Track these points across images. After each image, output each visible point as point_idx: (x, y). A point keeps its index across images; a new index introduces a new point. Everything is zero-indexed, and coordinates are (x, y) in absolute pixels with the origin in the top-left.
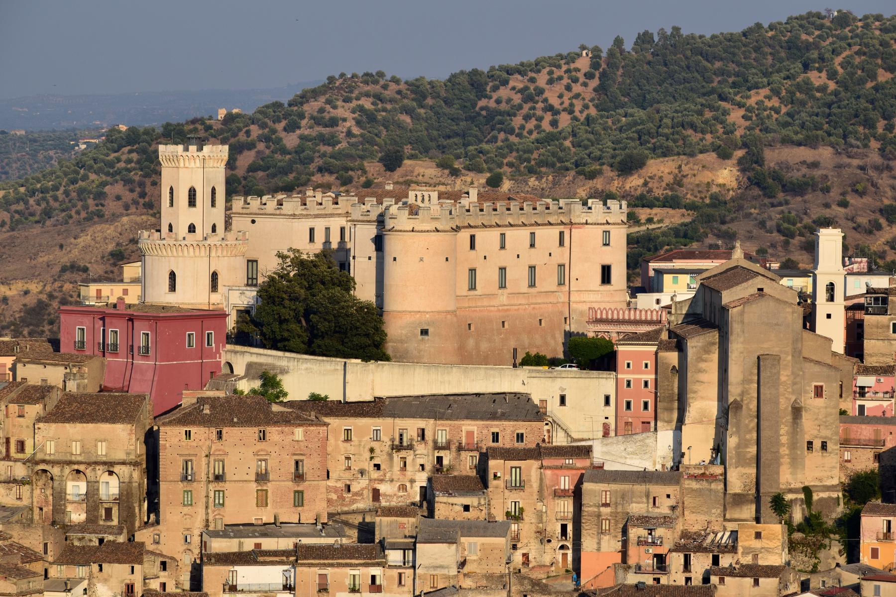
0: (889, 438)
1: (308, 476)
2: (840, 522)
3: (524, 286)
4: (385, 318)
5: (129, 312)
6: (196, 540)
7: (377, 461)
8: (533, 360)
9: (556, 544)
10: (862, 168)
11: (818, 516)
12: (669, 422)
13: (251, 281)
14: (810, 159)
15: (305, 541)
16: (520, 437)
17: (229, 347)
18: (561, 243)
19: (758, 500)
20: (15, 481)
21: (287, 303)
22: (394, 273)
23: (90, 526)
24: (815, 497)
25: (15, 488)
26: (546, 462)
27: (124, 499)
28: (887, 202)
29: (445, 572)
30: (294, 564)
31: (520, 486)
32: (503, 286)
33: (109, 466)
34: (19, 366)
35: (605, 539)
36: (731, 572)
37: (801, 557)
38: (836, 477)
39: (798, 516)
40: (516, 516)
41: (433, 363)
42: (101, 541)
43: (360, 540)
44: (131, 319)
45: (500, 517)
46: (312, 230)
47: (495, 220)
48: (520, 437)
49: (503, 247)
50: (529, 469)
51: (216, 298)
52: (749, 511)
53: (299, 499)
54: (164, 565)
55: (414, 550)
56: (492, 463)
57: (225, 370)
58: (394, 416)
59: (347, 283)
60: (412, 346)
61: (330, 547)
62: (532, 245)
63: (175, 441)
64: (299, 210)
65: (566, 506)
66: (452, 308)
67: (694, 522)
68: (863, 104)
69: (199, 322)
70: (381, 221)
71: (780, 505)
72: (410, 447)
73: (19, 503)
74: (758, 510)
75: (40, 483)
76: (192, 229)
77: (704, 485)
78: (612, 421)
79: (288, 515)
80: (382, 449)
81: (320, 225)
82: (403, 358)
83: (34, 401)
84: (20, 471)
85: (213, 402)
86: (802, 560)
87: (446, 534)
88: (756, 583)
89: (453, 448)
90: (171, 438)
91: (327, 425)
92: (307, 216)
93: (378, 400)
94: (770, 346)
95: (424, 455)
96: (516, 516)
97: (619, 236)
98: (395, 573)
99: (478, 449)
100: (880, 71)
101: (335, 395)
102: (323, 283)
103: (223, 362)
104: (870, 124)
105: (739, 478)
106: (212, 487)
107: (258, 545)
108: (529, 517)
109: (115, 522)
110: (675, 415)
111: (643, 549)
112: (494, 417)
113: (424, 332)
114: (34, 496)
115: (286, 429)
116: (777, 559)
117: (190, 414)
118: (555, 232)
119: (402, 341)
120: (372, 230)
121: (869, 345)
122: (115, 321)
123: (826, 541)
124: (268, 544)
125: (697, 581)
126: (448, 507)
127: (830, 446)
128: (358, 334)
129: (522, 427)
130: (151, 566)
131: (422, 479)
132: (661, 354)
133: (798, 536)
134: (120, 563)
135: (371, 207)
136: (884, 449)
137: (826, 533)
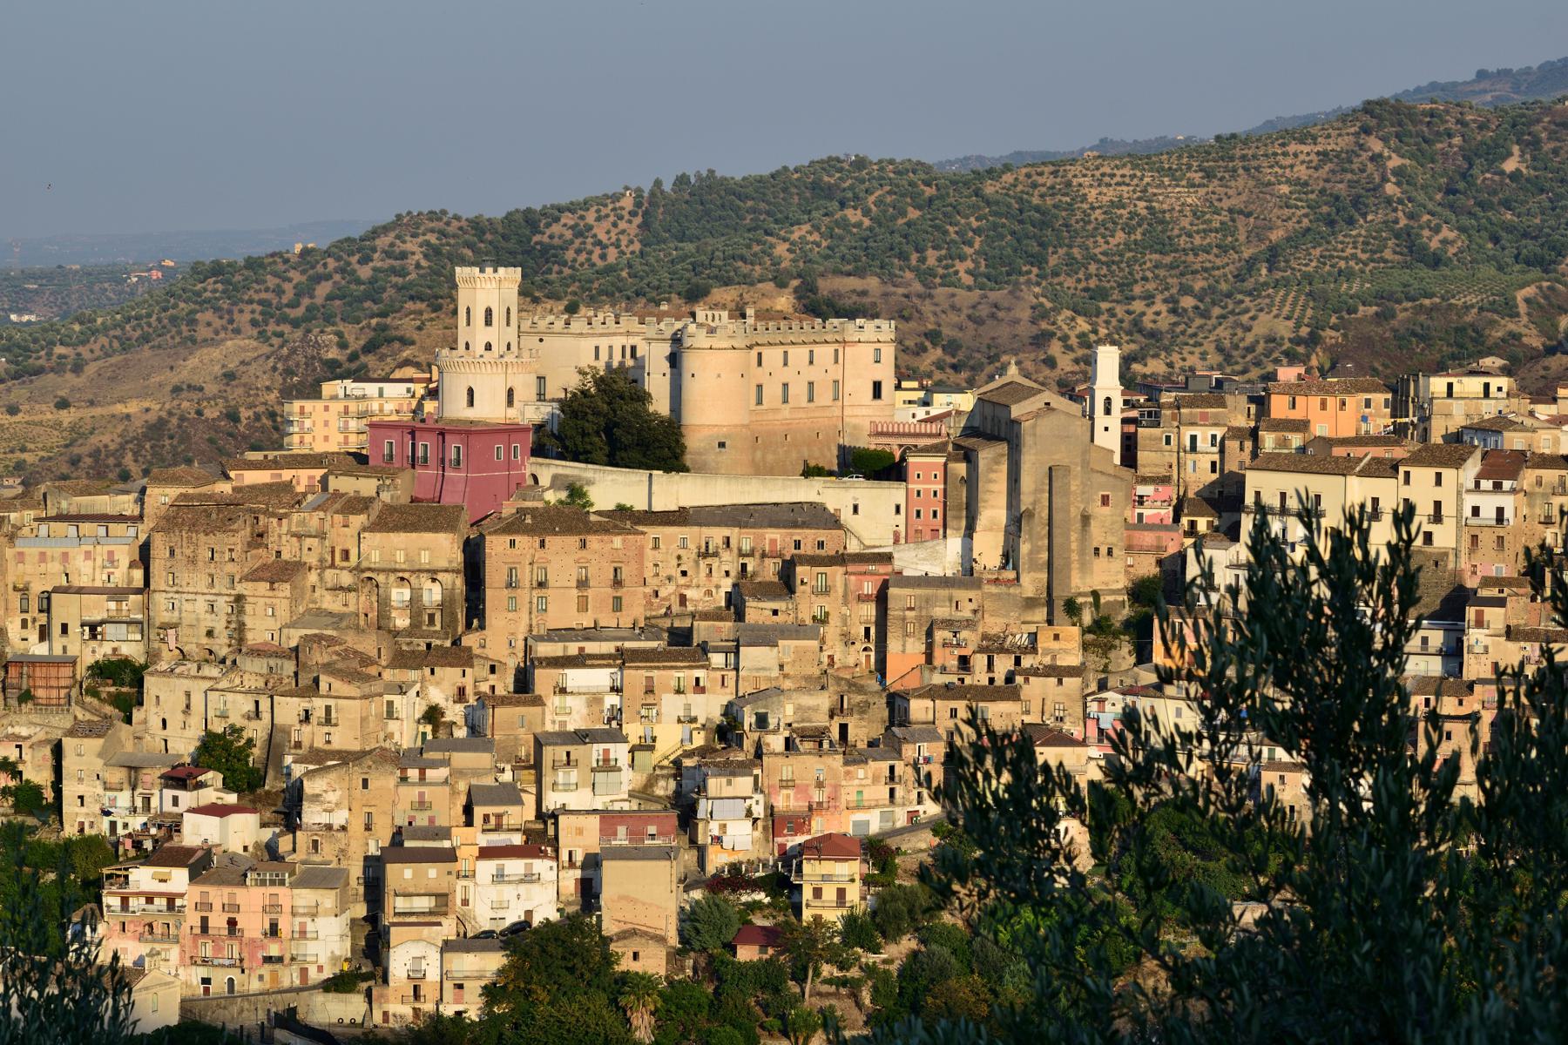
0: (1171, 544)
1: (627, 583)
2: (1128, 625)
3: (804, 402)
4: (683, 430)
5: (440, 425)
6: (521, 644)
7: (683, 568)
8: (810, 472)
9: (859, 646)
10: (907, 296)
11: (1107, 618)
12: (958, 529)
13: (541, 397)
14: (859, 289)
15: (628, 645)
16: (821, 545)
17: (533, 459)
18: (836, 362)
19: (1050, 603)
20: (341, 588)
21: (590, 418)
22: (694, 390)
23: (417, 631)
24: (1102, 601)
25: (341, 595)
26: (851, 568)
27: (446, 606)
28: (930, 327)
29: (767, 673)
30: (621, 667)
31: (826, 591)
32: (785, 401)
33: (433, 575)
34: (331, 478)
35: (910, 641)
36: (1035, 672)
37: (1093, 657)
38: (1122, 582)
39: (1087, 618)
40: (822, 620)
41: (731, 474)
42: (429, 646)
43: (670, 644)
44: (442, 433)
45: (809, 622)
46: (597, 348)
47: (779, 338)
48: (821, 545)
49: (786, 364)
50: (834, 577)
51: (512, 413)
52: (1041, 614)
53: (618, 604)
54: (493, 670)
55: (737, 653)
56: (799, 569)
57: (530, 482)
58: (700, 525)
59: (644, 397)
60: (711, 458)
61: (653, 650)
62: (811, 362)
63: (500, 549)
64: (586, 329)
65: (869, 610)
66: (746, 422)
67: (993, 624)
68: (897, 238)
69: (505, 436)
70: (677, 340)
71: (1072, 608)
72: (716, 554)
73: (345, 609)
74: (1050, 613)
75: (366, 590)
76: (488, 347)
77: (1003, 589)
78: (902, 529)
79: (608, 620)
80: (689, 556)
81: (604, 343)
82: (702, 469)
83: (361, 512)
84: (346, 579)
85: (533, 511)
86: (1095, 661)
87: (766, 637)
88: (1060, 682)
89: (757, 555)
90: (496, 546)
91: (643, 533)
92: (593, 335)
93: (682, 510)
94: (1060, 457)
95: (729, 562)
96: (822, 620)
97: (888, 352)
98: (718, 674)
99: (780, 556)
100: (910, 209)
101: (640, 505)
102: (622, 398)
103: (528, 473)
104: (904, 256)
105: (1032, 582)
106: (535, 593)
107: (582, 649)
108: (834, 620)
109: (438, 627)
110: (964, 523)
111: (948, 650)
112: (795, 525)
113: (722, 445)
114: (360, 603)
115: (606, 538)
116: (1073, 659)
117: (512, 523)
118: (830, 349)
119: (700, 454)
120: (666, 349)
121: (1142, 456)
122: (426, 435)
123: (1117, 642)
124: (592, 648)
125: (1000, 680)
126: (758, 612)
127: (1115, 552)
128: (660, 447)
129: (822, 535)
130: (480, 670)
131: (727, 585)
132: (950, 465)
133: (1090, 637)
134: (451, 666)
135: (669, 326)
136: (1166, 555)
137: (1116, 635)
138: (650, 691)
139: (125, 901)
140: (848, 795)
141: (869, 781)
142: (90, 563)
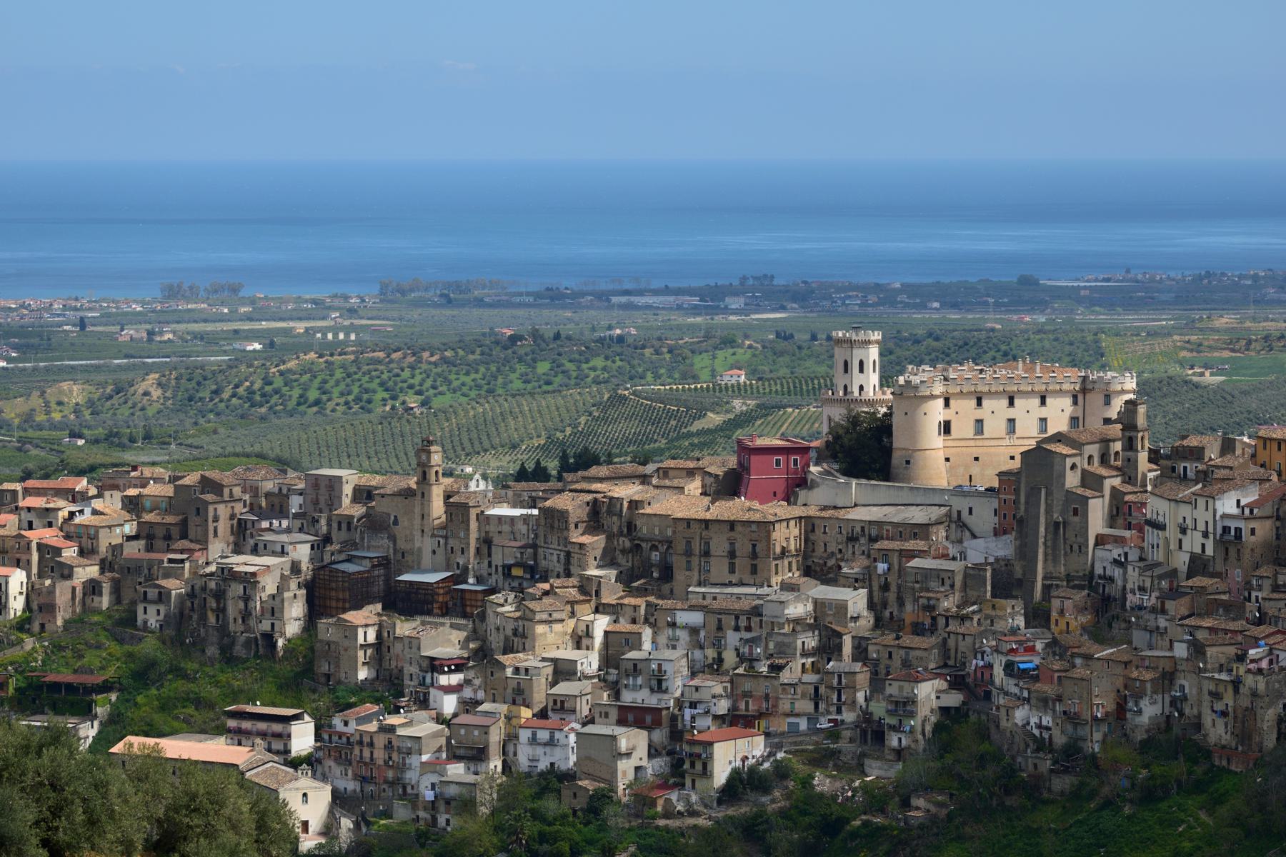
72: (857, 539)
108: (893, 588)
138: (720, 628)
139: (330, 737)
140: (785, 706)
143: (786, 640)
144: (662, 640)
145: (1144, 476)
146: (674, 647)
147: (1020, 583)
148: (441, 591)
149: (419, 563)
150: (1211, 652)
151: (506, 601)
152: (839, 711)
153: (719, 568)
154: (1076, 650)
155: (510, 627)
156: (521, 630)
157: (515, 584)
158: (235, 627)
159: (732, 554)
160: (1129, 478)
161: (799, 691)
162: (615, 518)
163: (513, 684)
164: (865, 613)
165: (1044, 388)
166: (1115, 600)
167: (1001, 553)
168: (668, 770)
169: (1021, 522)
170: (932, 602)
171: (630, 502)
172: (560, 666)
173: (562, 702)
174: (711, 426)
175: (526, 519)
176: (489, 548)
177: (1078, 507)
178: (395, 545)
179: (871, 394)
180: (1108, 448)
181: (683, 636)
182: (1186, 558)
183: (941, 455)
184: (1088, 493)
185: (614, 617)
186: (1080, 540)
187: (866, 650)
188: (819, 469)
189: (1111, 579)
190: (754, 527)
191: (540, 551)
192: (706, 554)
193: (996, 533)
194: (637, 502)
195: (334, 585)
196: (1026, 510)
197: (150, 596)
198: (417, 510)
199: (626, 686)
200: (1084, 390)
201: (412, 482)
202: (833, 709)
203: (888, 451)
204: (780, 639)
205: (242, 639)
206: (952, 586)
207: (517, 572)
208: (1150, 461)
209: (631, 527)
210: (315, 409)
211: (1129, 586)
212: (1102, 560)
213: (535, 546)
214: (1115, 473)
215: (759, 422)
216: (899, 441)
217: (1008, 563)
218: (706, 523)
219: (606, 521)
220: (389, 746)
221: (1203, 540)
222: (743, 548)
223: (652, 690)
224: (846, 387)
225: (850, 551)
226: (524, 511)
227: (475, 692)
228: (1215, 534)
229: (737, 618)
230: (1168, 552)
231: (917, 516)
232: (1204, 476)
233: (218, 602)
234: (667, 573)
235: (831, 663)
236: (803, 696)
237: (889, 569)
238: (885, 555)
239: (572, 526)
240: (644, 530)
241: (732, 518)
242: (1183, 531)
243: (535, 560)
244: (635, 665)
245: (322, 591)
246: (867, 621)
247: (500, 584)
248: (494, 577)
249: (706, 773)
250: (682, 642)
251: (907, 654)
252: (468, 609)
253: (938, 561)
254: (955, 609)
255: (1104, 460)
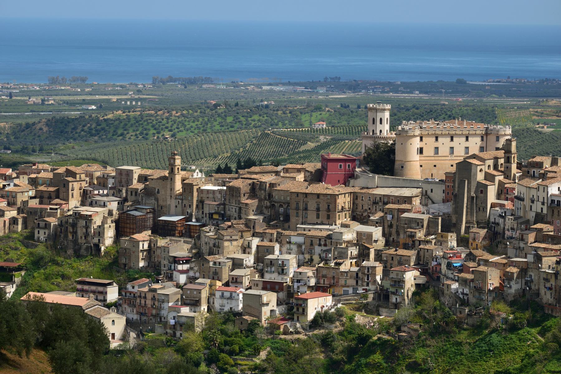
72: (378, 203)
108: (395, 227)
138: (312, 244)
139: (126, 293)
140: (342, 282)
141: (349, 278)
142: (220, 195)
143: (343, 251)
144: (284, 249)
145: (515, 175)
146: (290, 253)
147: (455, 225)
148: (179, 225)
149: (169, 212)
150: (544, 259)
151: (210, 230)
152: (368, 285)
153: (312, 216)
154: (481, 258)
155: (212, 242)
156: (217, 244)
157: (215, 222)
158: (81, 241)
159: (318, 210)
160: (507, 177)
161: (349, 275)
162: (263, 192)
163: (213, 270)
164: (381, 238)
165: (467, 132)
166: (500, 234)
167: (446, 211)
168: (286, 312)
169: (456, 196)
170: (413, 234)
171: (270, 184)
172: (235, 261)
173: (236, 279)
174: (309, 148)
175: (220, 191)
176: (203, 205)
177: (482, 189)
178: (158, 202)
179: (386, 134)
180: (497, 162)
181: (294, 247)
182: (534, 214)
183: (418, 164)
184: (488, 183)
185: (261, 239)
186: (483, 205)
187: (381, 256)
188: (360, 169)
189: (498, 224)
190: (329, 197)
191: (227, 206)
192: (306, 209)
193: (444, 201)
194: (273, 184)
195: (128, 221)
196: (458, 191)
197: (41, 225)
198: (169, 186)
199: (267, 272)
200: (487, 134)
201: (166, 173)
202: (365, 284)
203: (393, 162)
204: (340, 250)
205: (85, 246)
206: (423, 226)
207: (216, 216)
208: (518, 168)
209: (270, 196)
210: (121, 138)
211: (506, 227)
212: (494, 215)
213: (224, 204)
214: (501, 174)
215: (332, 147)
216: (398, 157)
217: (449, 215)
218: (306, 195)
219: (258, 193)
220: (154, 298)
221: (542, 206)
222: (323, 206)
223: (279, 274)
224: (373, 131)
225: (374, 209)
226: (219, 188)
227: (195, 273)
228: (547, 203)
229: (320, 240)
230: (525, 212)
231: (406, 192)
232: (543, 176)
233: (73, 229)
234: (287, 218)
235: (364, 262)
236: (351, 277)
237: (393, 218)
238: (391, 211)
239: (243, 195)
240: (277, 198)
241: (318, 192)
242: (533, 202)
243: (225, 211)
244: (271, 262)
245: (123, 224)
246: (381, 243)
247: (208, 222)
248: (205, 219)
249: (304, 312)
250: (294, 251)
251: (401, 258)
252: (192, 234)
253: (416, 214)
254: (423, 237)
255: (496, 167)
